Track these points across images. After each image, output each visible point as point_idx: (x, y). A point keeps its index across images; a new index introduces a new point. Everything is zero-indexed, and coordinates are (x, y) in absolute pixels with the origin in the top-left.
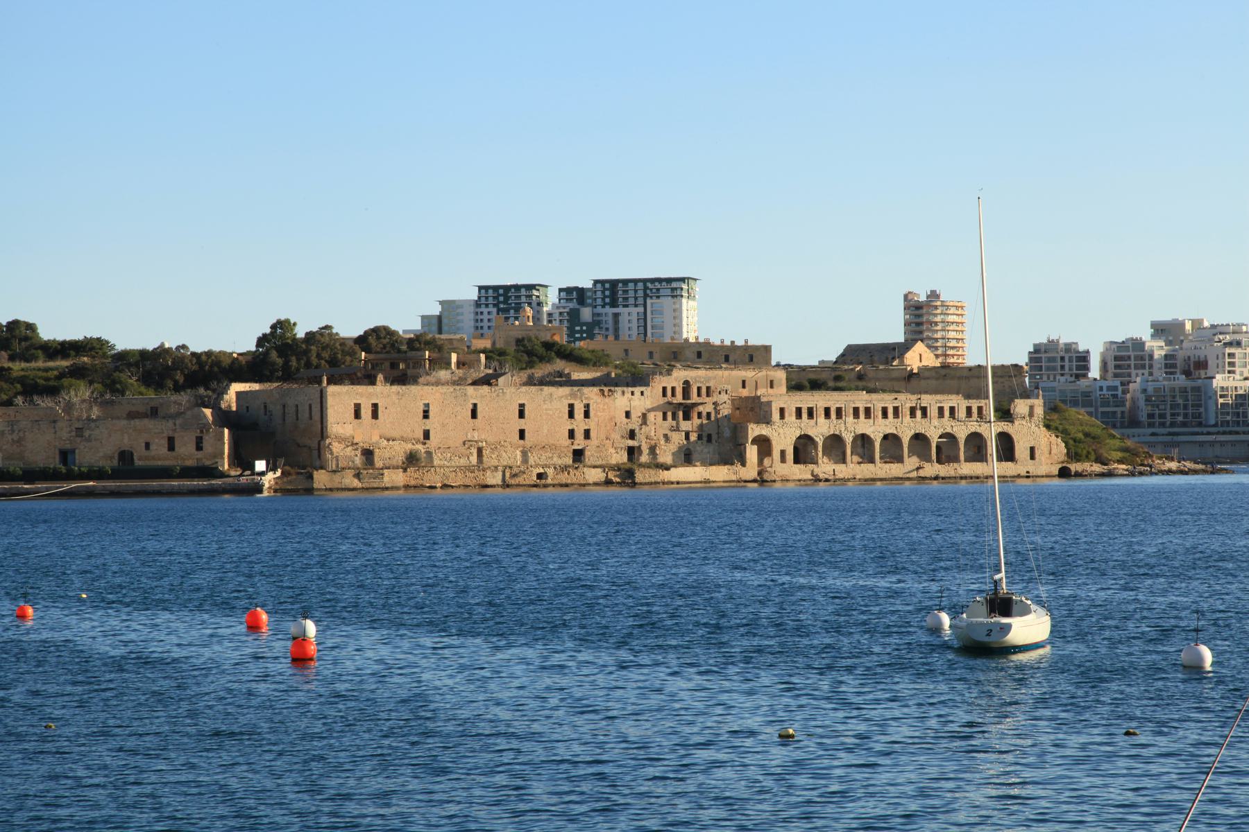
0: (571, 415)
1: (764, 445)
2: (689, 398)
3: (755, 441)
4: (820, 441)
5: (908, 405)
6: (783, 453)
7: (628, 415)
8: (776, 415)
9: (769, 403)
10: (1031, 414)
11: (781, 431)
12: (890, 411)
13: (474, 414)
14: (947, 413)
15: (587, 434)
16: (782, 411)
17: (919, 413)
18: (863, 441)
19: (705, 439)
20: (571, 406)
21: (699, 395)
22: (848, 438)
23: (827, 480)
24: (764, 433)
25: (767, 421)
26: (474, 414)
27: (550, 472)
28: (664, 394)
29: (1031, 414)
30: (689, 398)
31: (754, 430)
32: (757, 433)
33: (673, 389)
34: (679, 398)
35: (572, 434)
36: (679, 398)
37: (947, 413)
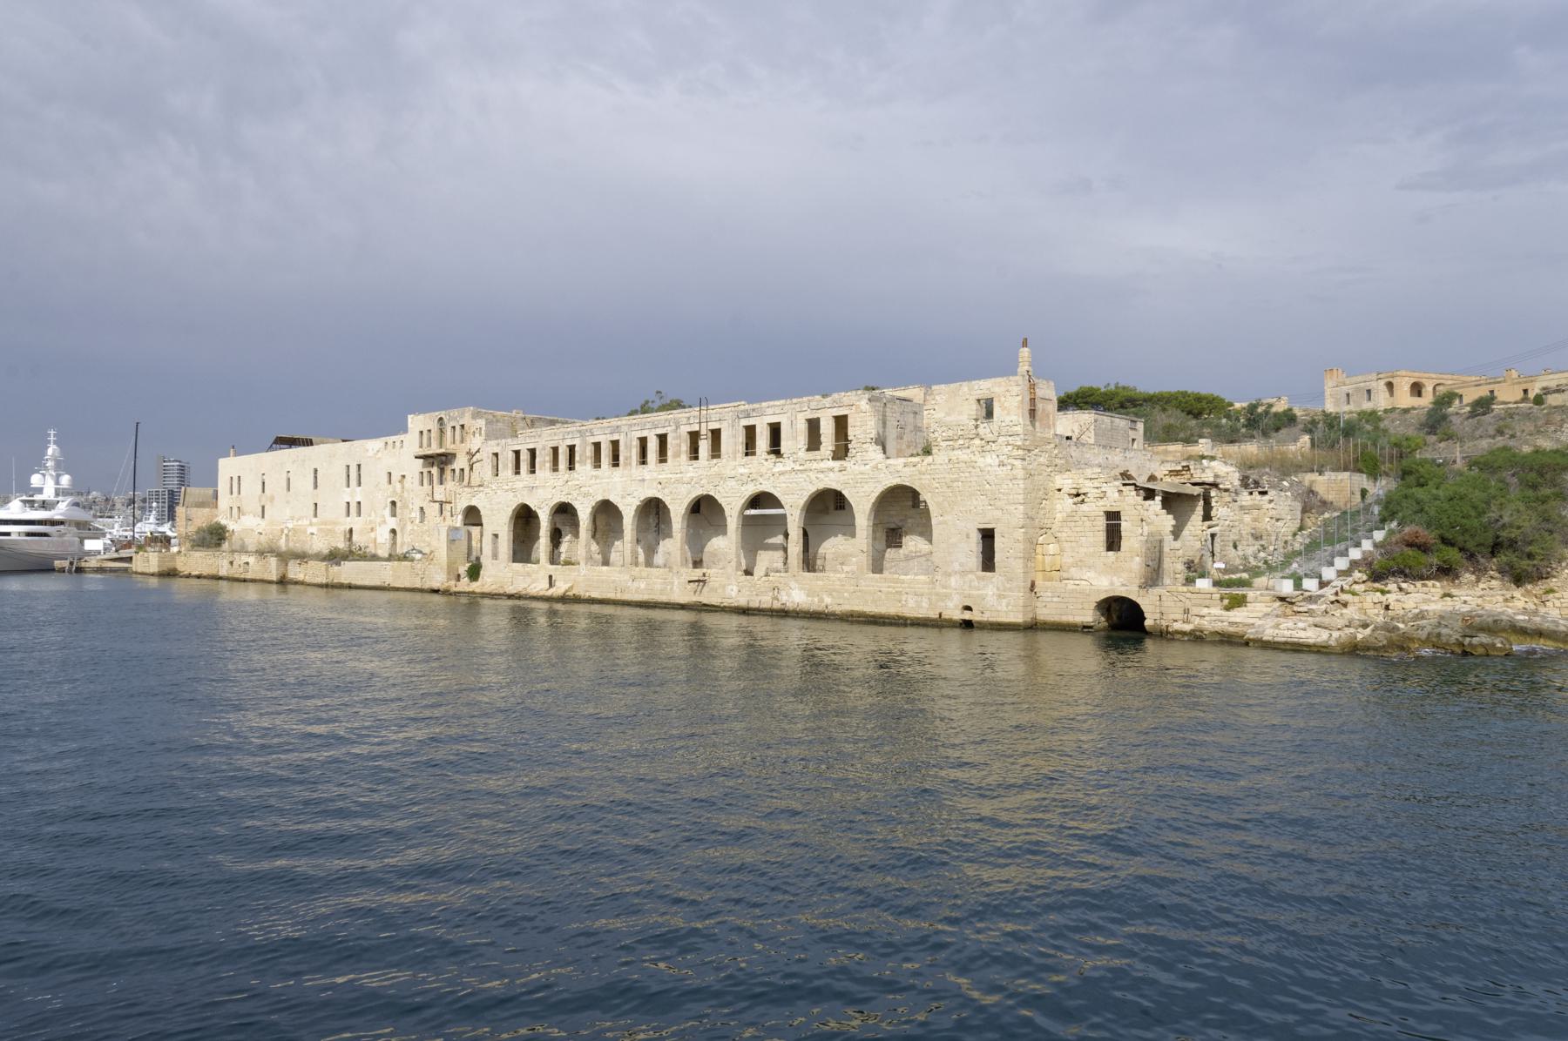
5: (685, 430)
17: (704, 446)
34: (435, 449)
37: (763, 442)
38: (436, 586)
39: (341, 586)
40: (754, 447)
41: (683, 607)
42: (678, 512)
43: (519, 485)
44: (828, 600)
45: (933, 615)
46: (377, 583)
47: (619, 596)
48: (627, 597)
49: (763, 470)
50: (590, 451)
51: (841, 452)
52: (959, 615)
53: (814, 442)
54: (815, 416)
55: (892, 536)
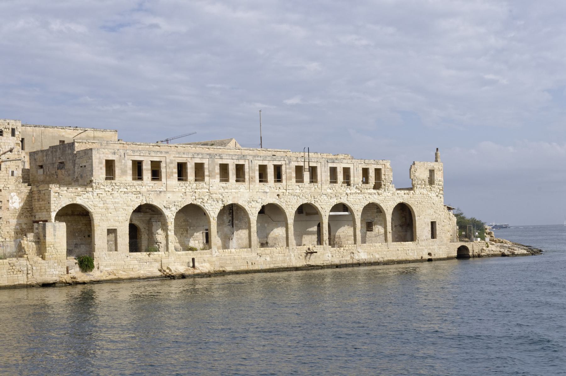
1: (78, 219)
3: (63, 214)
4: (170, 215)
5: (294, 164)
8: (99, 173)
9: (88, 153)
10: (431, 181)
11: (109, 199)
14: (340, 177)
16: (110, 165)
17: (307, 176)
18: (232, 214)
22: (213, 211)
23: (183, 276)
25: (83, 180)
29: (431, 181)
31: (61, 197)
32: (65, 202)
37: (340, 177)
38: (50, 279)
40: (266, 177)
41: (297, 269)
43: (144, 189)
44: (377, 256)
45: (419, 258)
47: (251, 268)
48: (256, 267)
49: (341, 191)
50: (217, 170)
51: (377, 186)
52: (427, 257)
53: (366, 181)
54: (367, 167)
55: (369, 226)
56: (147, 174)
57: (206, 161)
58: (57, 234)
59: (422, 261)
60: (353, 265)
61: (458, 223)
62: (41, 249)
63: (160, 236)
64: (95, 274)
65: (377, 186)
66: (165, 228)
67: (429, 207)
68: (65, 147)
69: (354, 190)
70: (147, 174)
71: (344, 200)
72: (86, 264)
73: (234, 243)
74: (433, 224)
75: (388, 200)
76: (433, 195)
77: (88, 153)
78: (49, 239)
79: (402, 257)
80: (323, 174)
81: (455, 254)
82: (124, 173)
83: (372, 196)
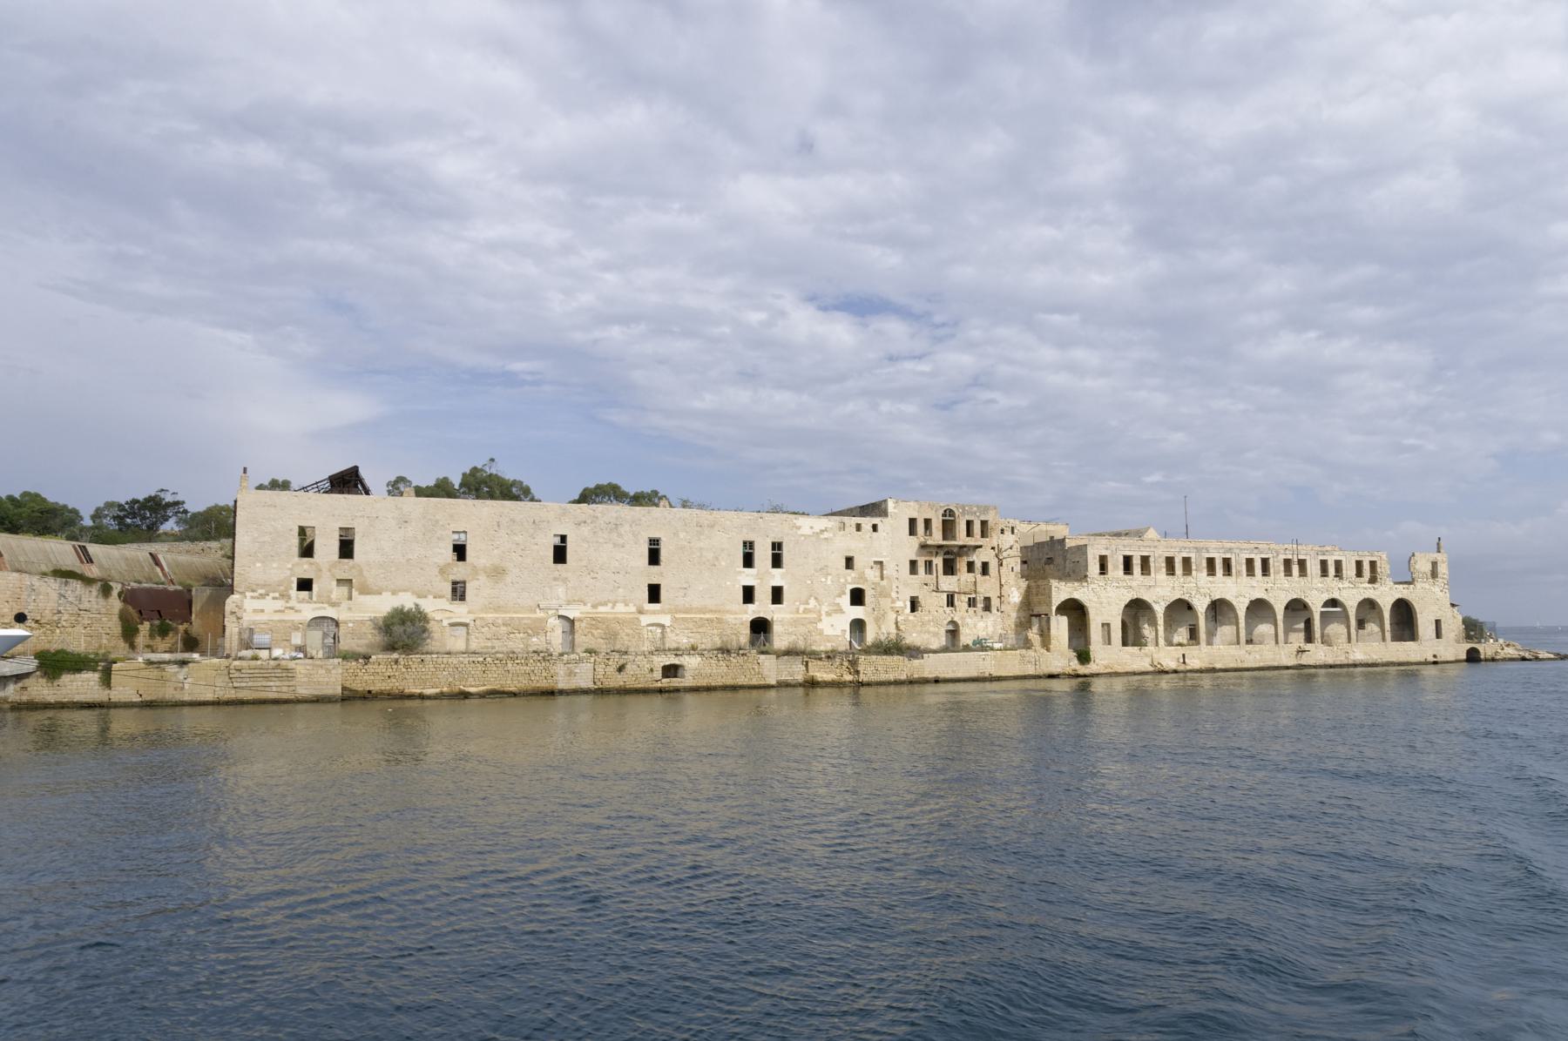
0: (748, 561)
1: (1076, 611)
2: (954, 538)
4: (1160, 610)
6: (1106, 626)
7: (849, 562)
9: (1082, 549)
10: (1434, 574)
12: (1258, 565)
13: (560, 555)
14: (1332, 570)
15: (777, 595)
17: (1295, 569)
18: (1219, 609)
19: (980, 605)
20: (748, 545)
21: (969, 533)
22: (1201, 605)
23: (1175, 672)
24: (1076, 596)
26: (560, 555)
27: (690, 662)
28: (912, 532)
29: (1434, 574)
30: (954, 538)
31: (1061, 591)
32: (1063, 597)
33: (927, 522)
34: (937, 538)
35: (749, 594)
36: (937, 538)
37: (1332, 570)
38: (1055, 671)
39: (925, 681)
41: (1288, 668)
42: (1241, 609)
46: (974, 674)
47: (1240, 665)
48: (1246, 665)
51: (1373, 580)
53: (1359, 574)
55: (1361, 624)
56: (1137, 569)
57: (1192, 555)
58: (1060, 627)
59: (1426, 663)
60: (1348, 666)
61: (1464, 622)
62: (1046, 644)
63: (1147, 631)
64: (1092, 668)
65: (1373, 580)
66: (1153, 623)
67: (1431, 602)
68: (1056, 544)
69: (1347, 584)
70: (1137, 569)
71: (1336, 596)
72: (1084, 657)
73: (1217, 639)
74: (1438, 622)
75: (1386, 595)
76: (1437, 589)
77: (1082, 549)
78: (1053, 632)
79: (1403, 658)
80: (1313, 567)
81: (1464, 657)
82: (1116, 567)
83: (1365, 590)
